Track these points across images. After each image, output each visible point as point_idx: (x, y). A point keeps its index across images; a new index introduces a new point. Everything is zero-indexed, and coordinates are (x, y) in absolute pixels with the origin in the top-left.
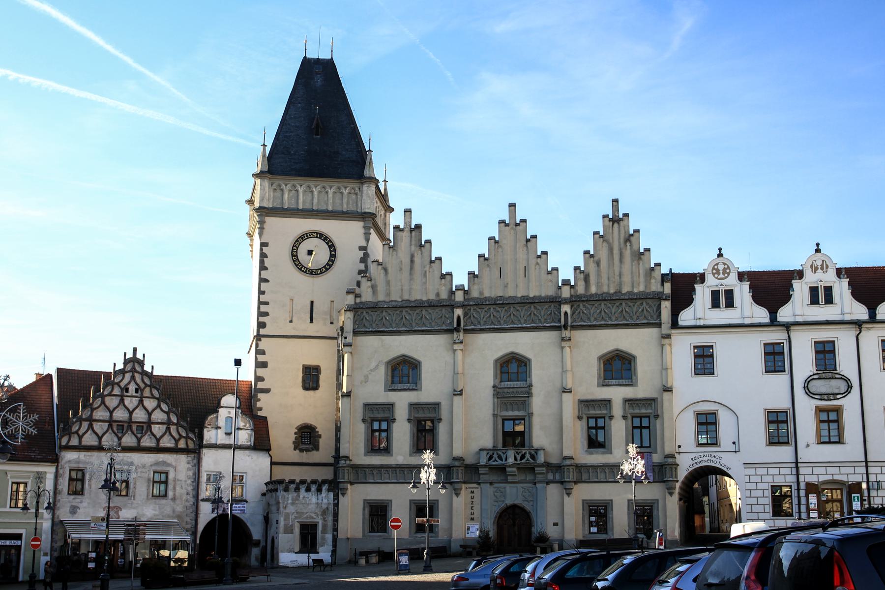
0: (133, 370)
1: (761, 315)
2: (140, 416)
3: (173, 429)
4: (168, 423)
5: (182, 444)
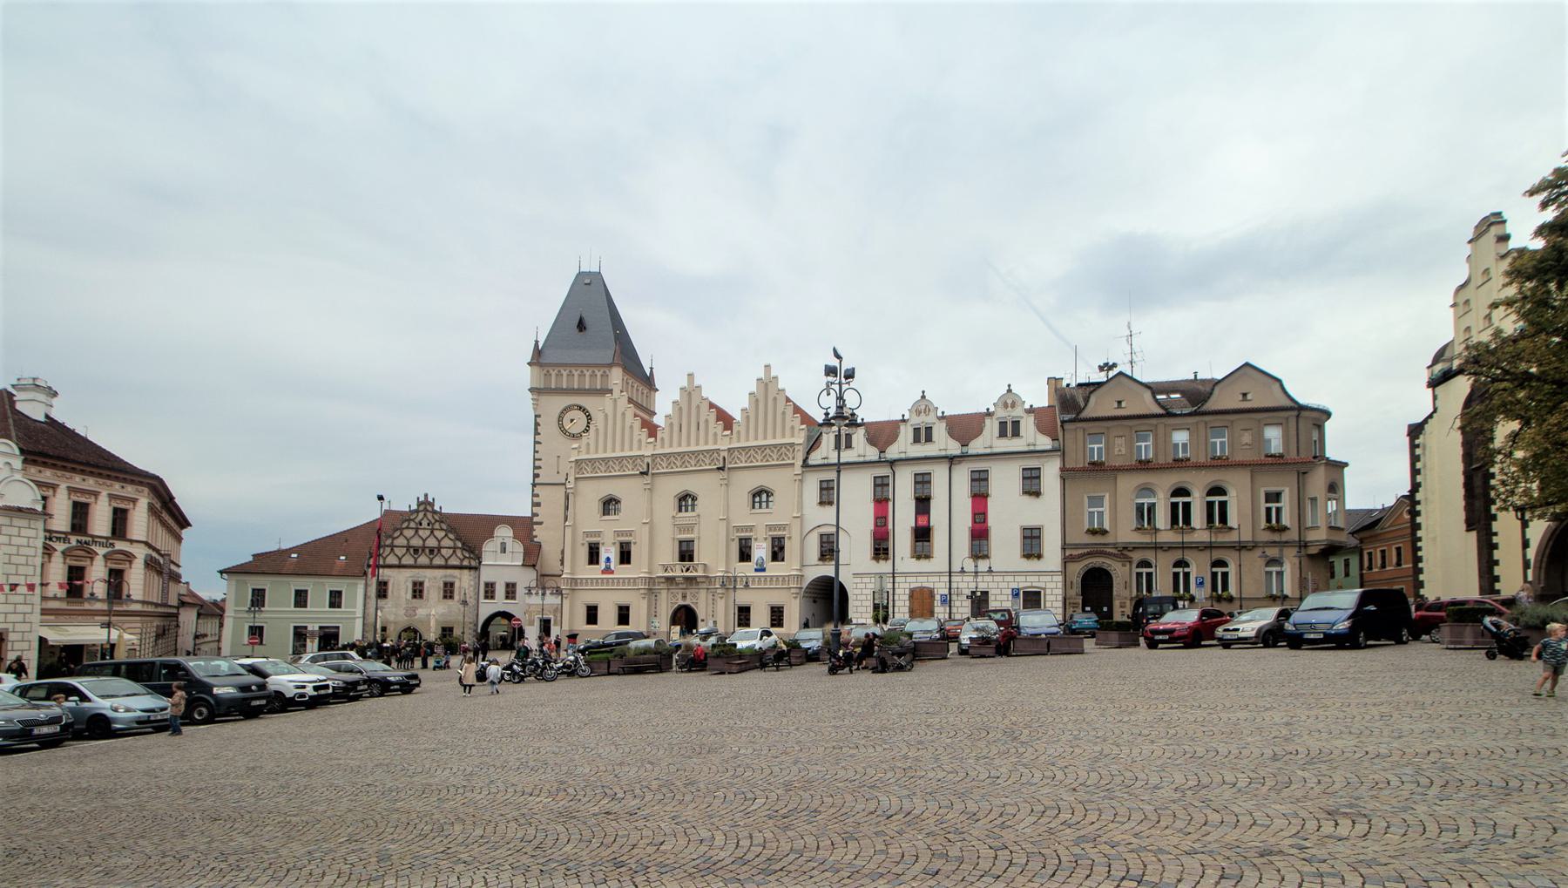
0: (426, 510)
1: (872, 453)
2: (432, 542)
3: (459, 552)
4: (455, 548)
5: (466, 563)
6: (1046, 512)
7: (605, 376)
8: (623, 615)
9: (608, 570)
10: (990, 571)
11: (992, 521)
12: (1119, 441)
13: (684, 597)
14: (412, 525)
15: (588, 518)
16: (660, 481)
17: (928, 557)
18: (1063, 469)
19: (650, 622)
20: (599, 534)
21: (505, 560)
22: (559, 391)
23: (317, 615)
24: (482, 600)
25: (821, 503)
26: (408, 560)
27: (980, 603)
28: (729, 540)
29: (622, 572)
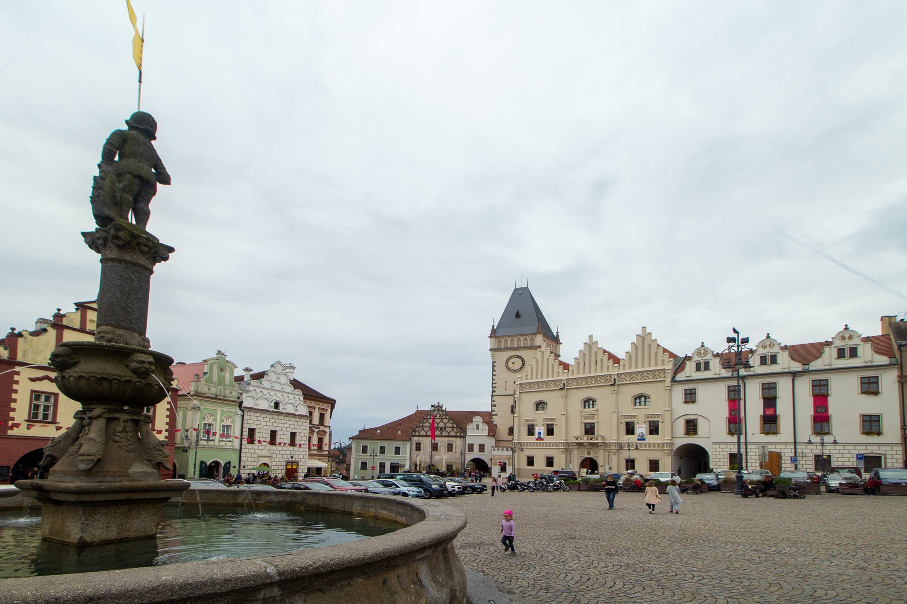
2: (441, 425)
4: (453, 427)
7: (532, 339)
8: (550, 462)
9: (539, 439)
10: (835, 442)
13: (589, 453)
15: (527, 410)
17: (775, 433)
19: (567, 466)
22: (506, 349)
25: (686, 402)
27: (823, 462)
28: (618, 424)
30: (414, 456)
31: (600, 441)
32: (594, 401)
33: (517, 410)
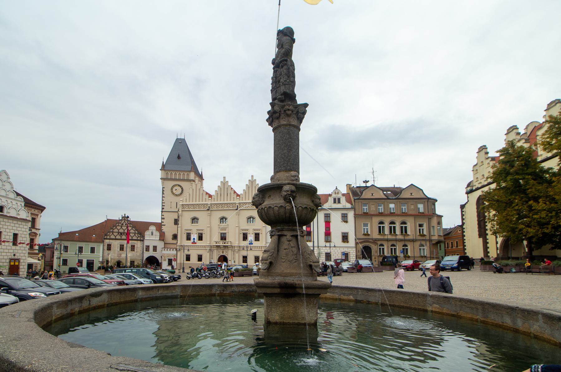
3: (136, 235)
4: (135, 233)
5: (139, 238)
6: (350, 228)
9: (194, 243)
11: (332, 230)
12: (372, 206)
13: (223, 252)
14: (120, 225)
16: (214, 213)
18: (355, 214)
20: (191, 230)
21: (153, 238)
23: (86, 256)
24: (145, 252)
26: (118, 237)
29: (199, 243)
30: (106, 254)
31: (229, 244)
32: (226, 219)
33: (180, 222)
